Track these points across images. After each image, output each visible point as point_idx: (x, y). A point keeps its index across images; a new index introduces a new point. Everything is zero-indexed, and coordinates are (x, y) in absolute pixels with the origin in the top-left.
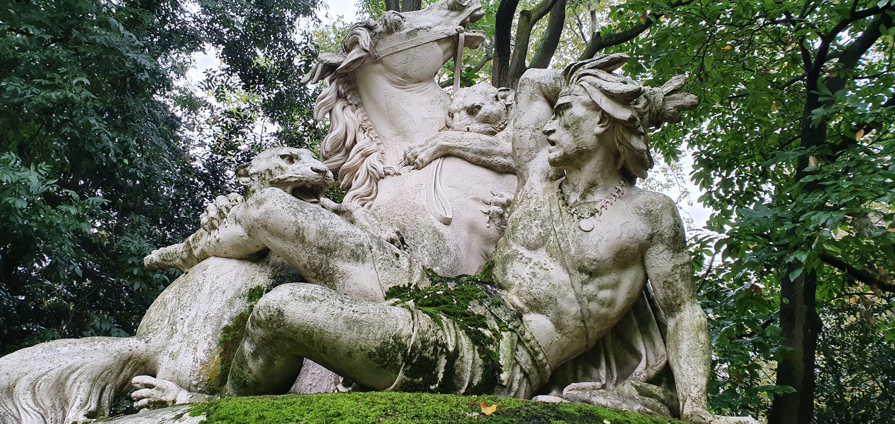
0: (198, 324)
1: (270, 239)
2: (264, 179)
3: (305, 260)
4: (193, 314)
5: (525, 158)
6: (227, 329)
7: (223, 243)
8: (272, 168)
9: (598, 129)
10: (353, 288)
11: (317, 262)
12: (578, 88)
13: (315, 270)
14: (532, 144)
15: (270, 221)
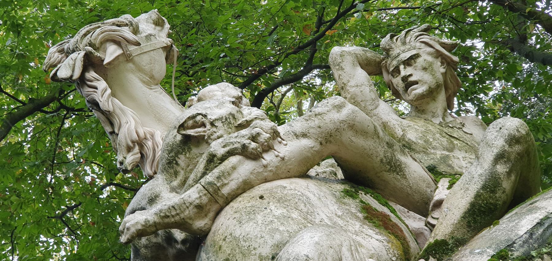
0: (340, 222)
1: (353, 139)
2: (230, 123)
3: (382, 154)
4: (324, 217)
5: (370, 108)
6: (366, 218)
7: (290, 160)
8: (234, 112)
9: (443, 70)
10: (416, 175)
11: (389, 154)
12: (418, 44)
13: (389, 163)
14: (373, 97)
15: (358, 119)
